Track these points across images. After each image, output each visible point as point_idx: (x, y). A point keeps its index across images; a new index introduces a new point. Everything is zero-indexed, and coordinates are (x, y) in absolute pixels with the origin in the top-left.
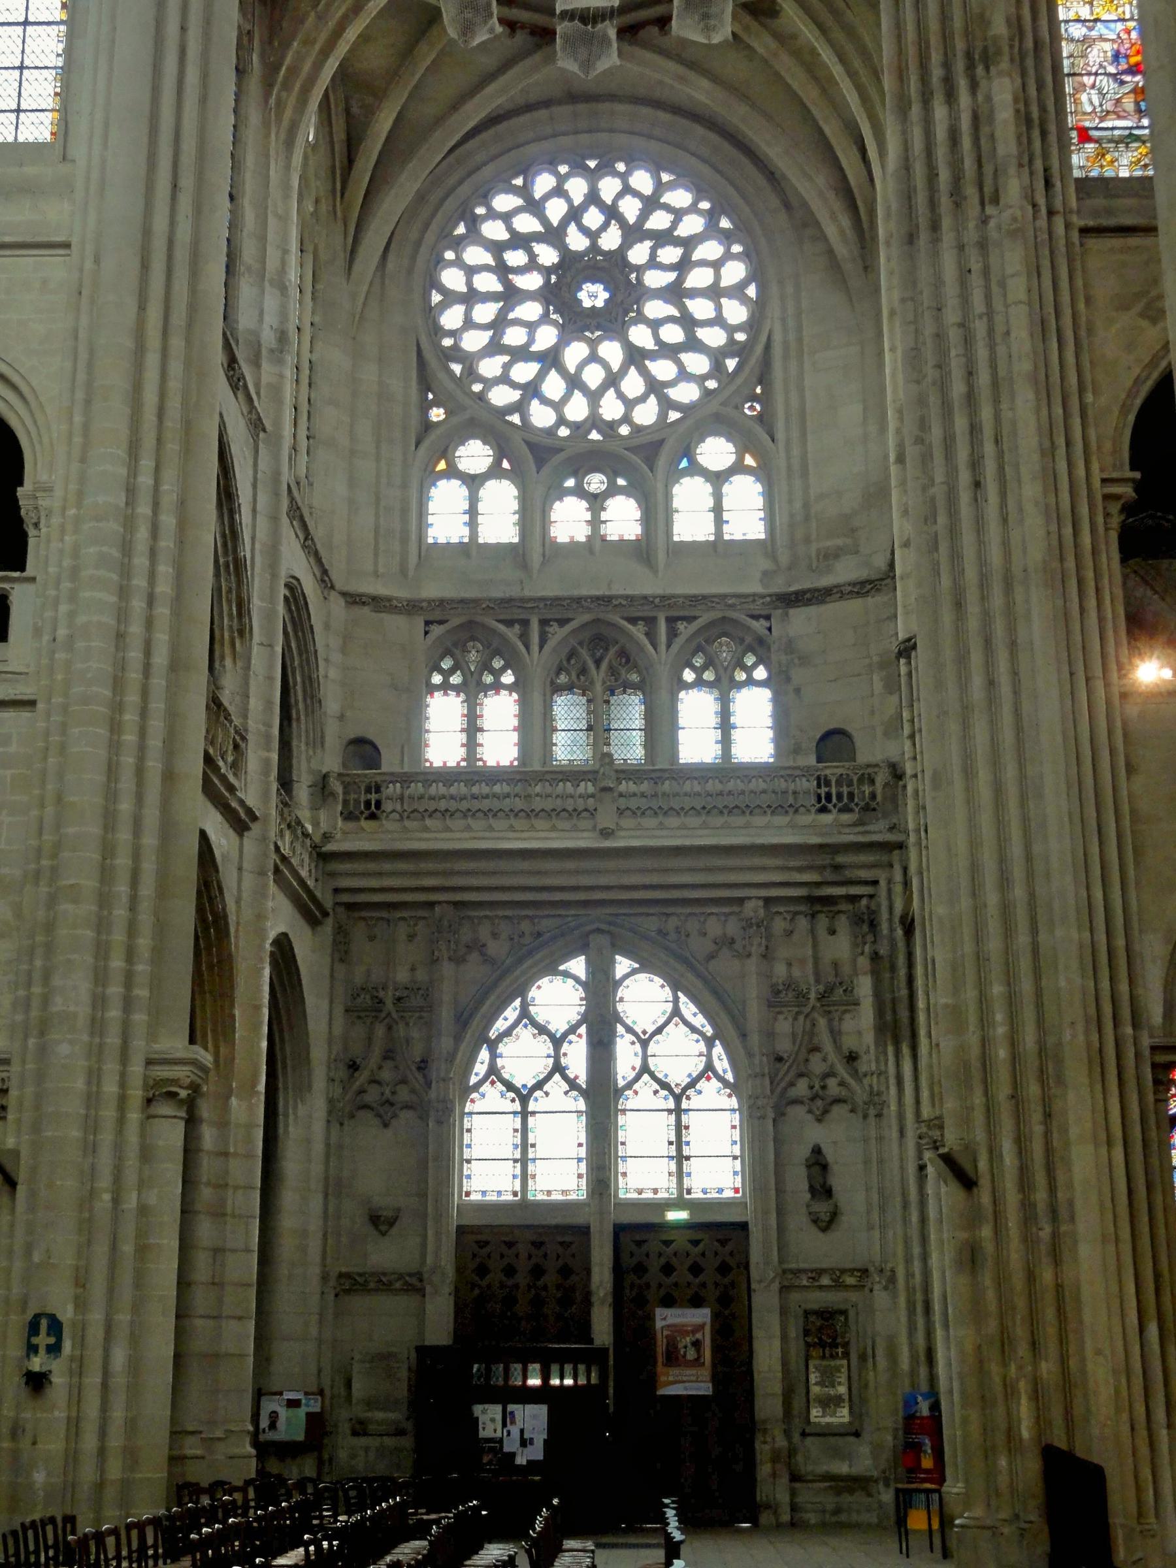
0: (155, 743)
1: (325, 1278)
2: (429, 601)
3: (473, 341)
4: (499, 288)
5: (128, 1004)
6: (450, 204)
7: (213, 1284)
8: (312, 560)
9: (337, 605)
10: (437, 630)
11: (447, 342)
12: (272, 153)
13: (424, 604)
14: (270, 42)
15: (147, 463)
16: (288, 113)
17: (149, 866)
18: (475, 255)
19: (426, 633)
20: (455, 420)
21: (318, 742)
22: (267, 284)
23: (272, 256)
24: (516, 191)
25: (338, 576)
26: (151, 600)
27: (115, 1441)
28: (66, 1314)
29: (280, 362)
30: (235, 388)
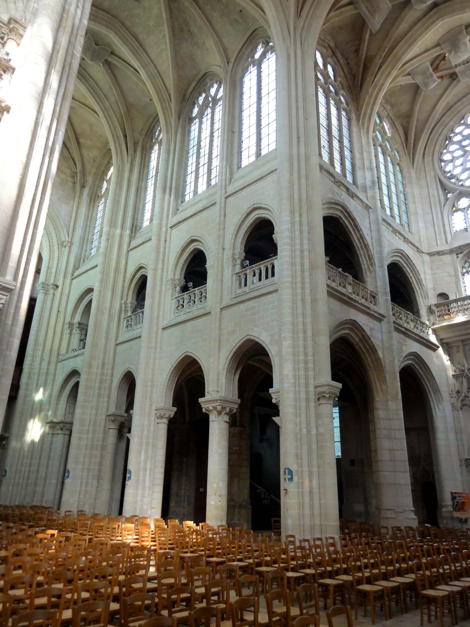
0: (308, 291)
1: (461, 461)
2: (456, 248)
3: (456, 172)
4: (462, 153)
5: (306, 369)
6: (442, 138)
7: (391, 461)
8: (409, 245)
9: (427, 258)
10: (460, 256)
11: (449, 175)
12: (362, 136)
13: (455, 249)
14: (358, 110)
15: (297, 214)
16: (366, 125)
17: (309, 327)
18: (453, 148)
19: (457, 257)
20: (455, 194)
21: (426, 297)
22: (366, 170)
23: (367, 163)
24: (462, 124)
25: (425, 248)
26: (302, 251)
27: (316, 511)
28: (294, 468)
29: (374, 189)
30: (352, 197)
